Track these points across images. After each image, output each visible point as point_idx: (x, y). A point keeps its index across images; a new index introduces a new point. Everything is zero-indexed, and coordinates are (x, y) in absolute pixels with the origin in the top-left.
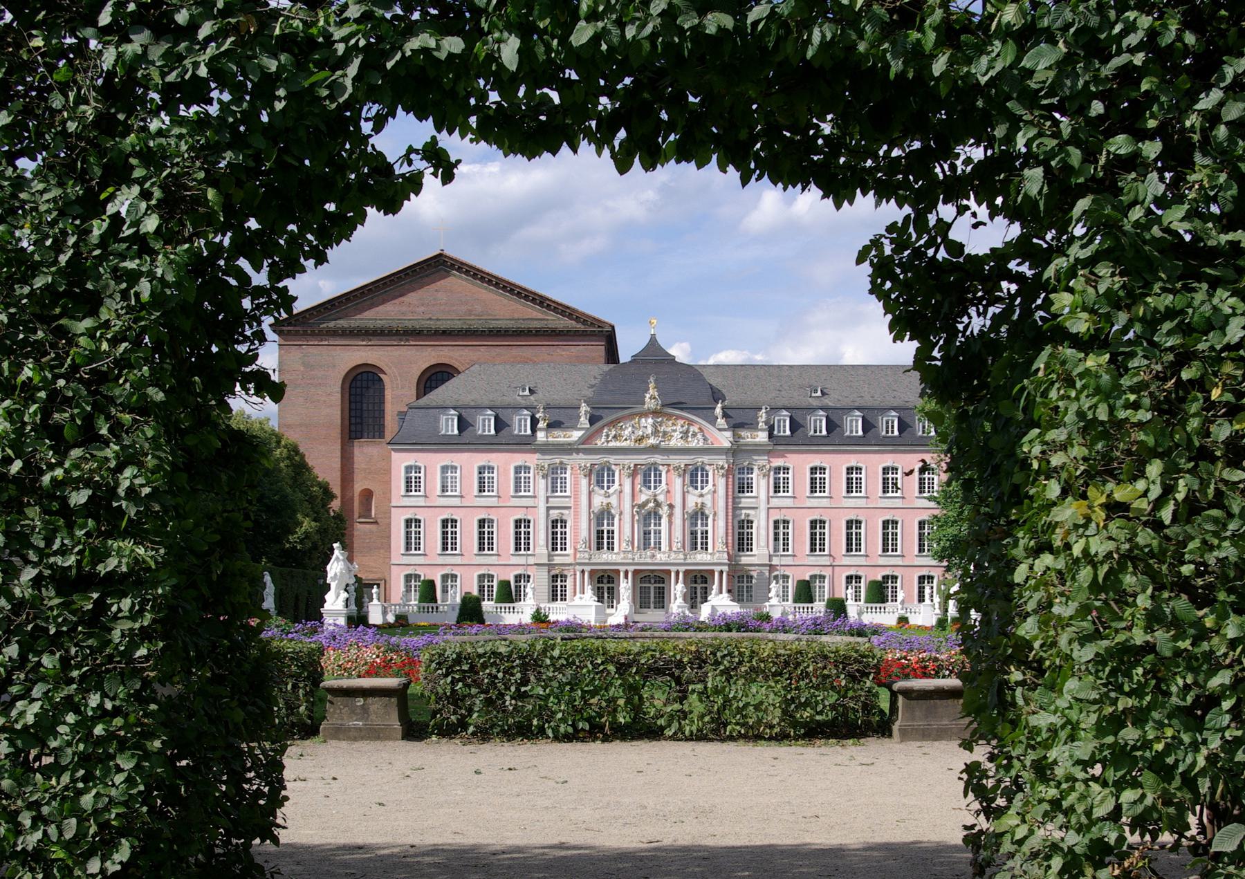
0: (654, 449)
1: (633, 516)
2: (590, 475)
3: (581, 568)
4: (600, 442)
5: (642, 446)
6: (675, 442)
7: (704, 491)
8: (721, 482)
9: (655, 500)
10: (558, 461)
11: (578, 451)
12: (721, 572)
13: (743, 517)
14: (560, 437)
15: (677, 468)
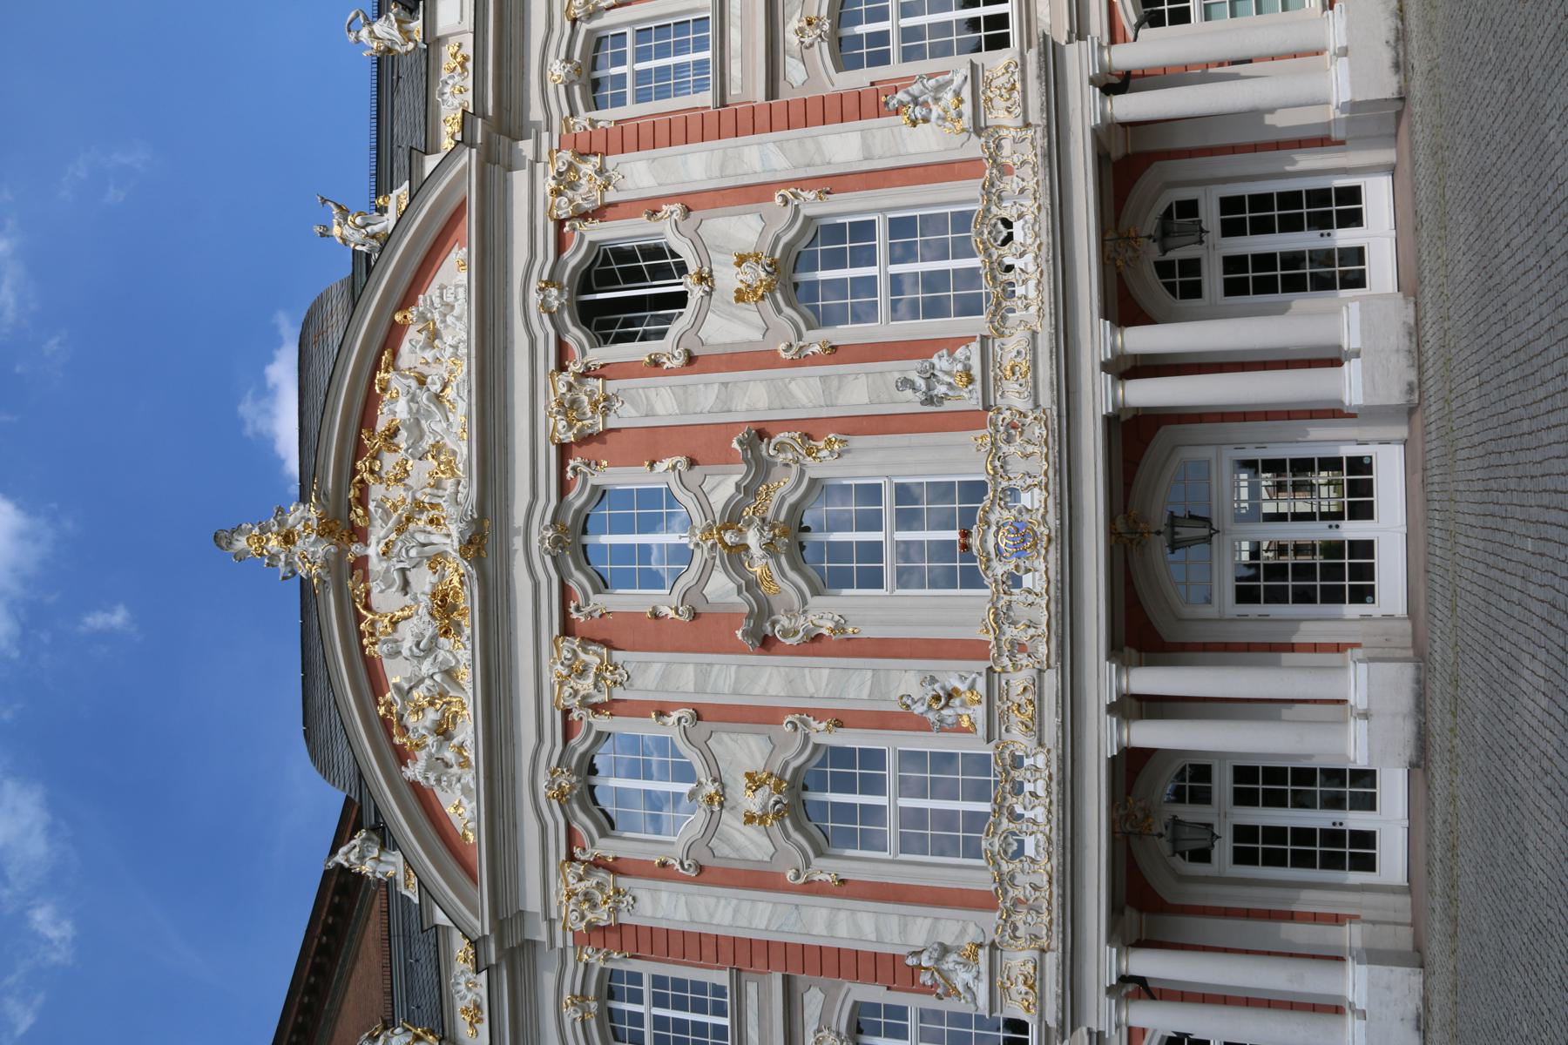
0: (485, 541)
1: (814, 643)
2: (615, 868)
3: (1100, 1012)
4: (462, 808)
5: (468, 601)
6: (455, 428)
7: (693, 267)
8: (638, 174)
9: (732, 518)
10: (570, 1014)
11: (507, 918)
12: (1115, 84)
13: (822, 54)
14: (467, 987)
15: (569, 408)
